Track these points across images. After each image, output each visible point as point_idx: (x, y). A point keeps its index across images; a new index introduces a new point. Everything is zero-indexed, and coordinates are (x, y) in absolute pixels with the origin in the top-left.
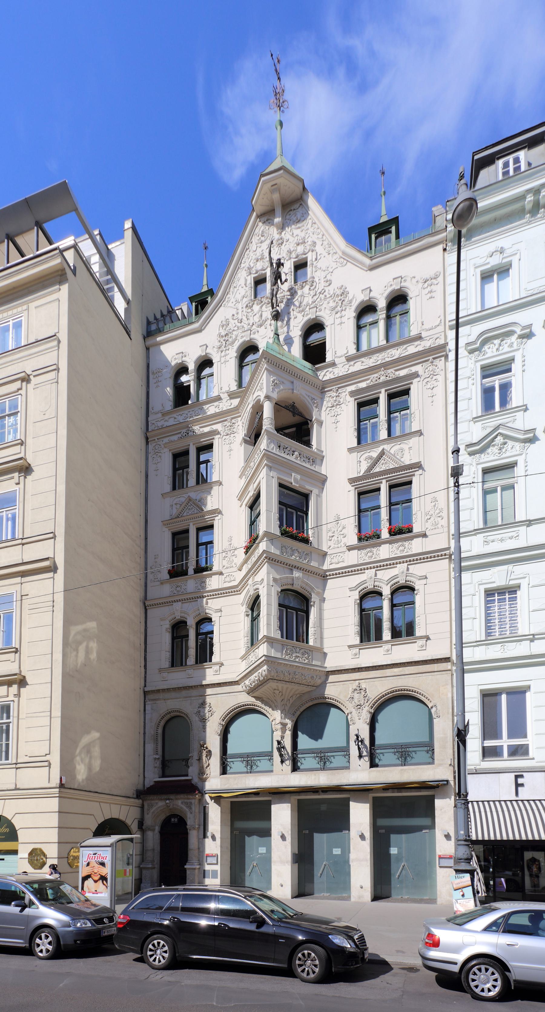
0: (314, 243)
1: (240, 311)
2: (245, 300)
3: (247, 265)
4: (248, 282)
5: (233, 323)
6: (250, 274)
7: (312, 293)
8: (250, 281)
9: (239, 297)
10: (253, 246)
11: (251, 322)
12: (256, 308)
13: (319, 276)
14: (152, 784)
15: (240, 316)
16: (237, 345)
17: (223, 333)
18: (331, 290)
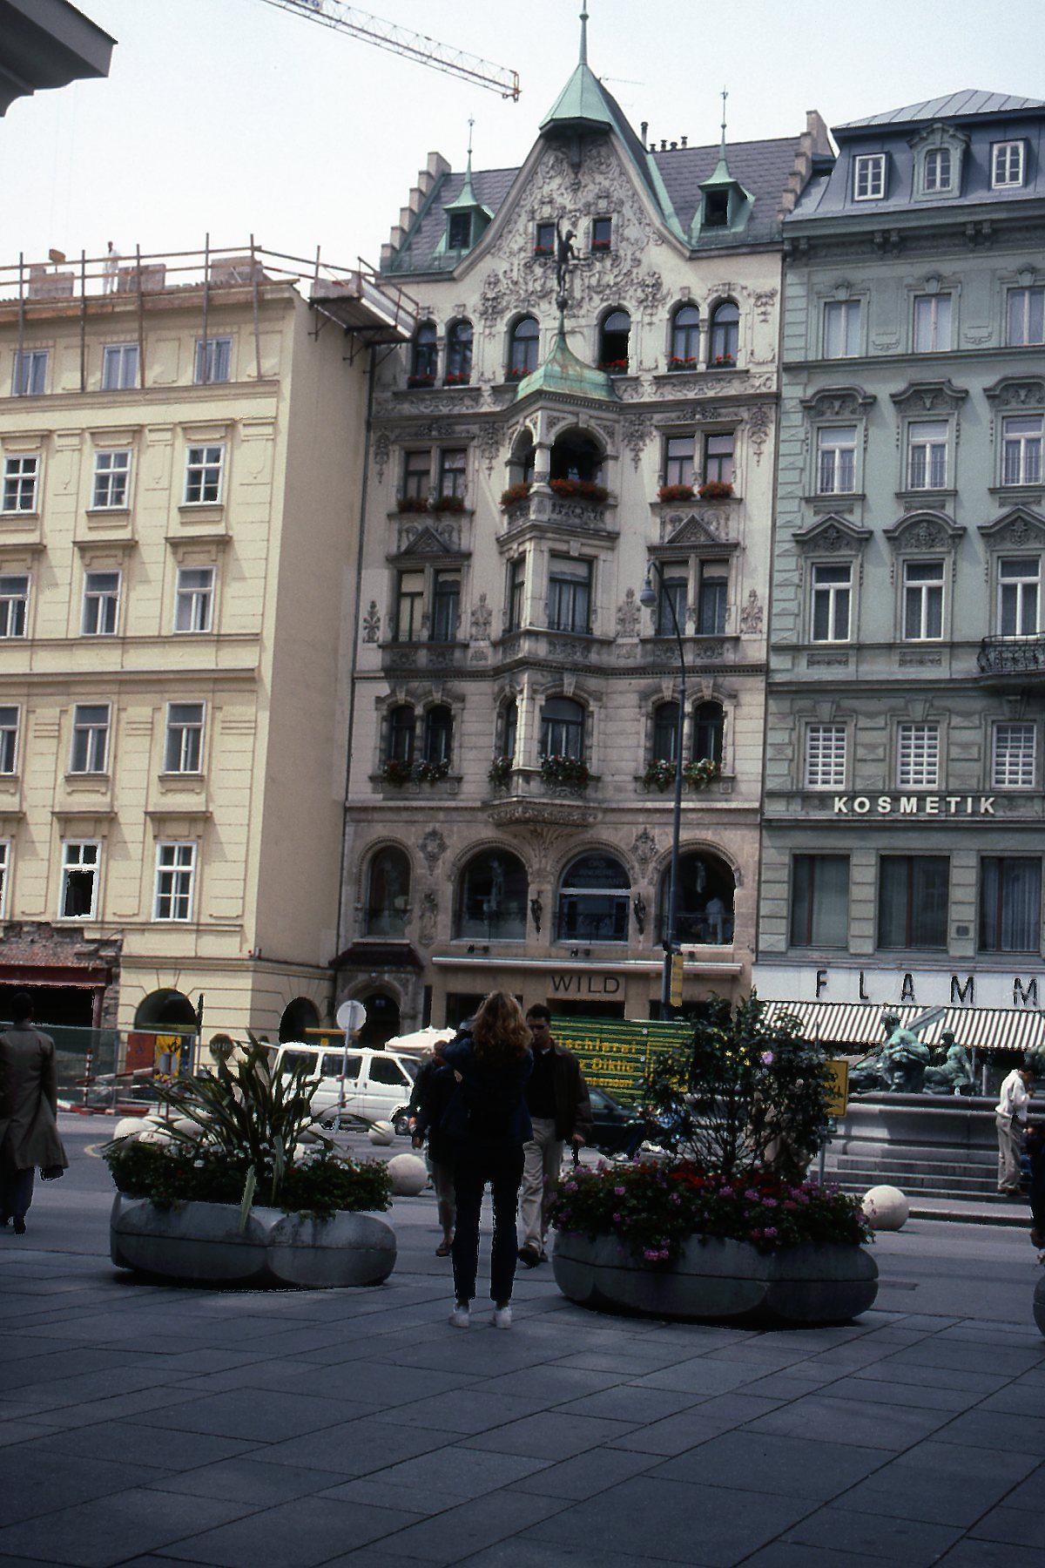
0: (622, 203)
1: (515, 268)
2: (523, 254)
3: (528, 208)
4: (530, 230)
5: (504, 285)
6: (533, 219)
7: (616, 271)
8: (532, 227)
9: (516, 247)
10: (539, 180)
11: (531, 289)
12: (538, 271)
13: (625, 251)
14: (350, 946)
15: (515, 275)
16: (508, 316)
17: (490, 295)
18: (640, 273)
